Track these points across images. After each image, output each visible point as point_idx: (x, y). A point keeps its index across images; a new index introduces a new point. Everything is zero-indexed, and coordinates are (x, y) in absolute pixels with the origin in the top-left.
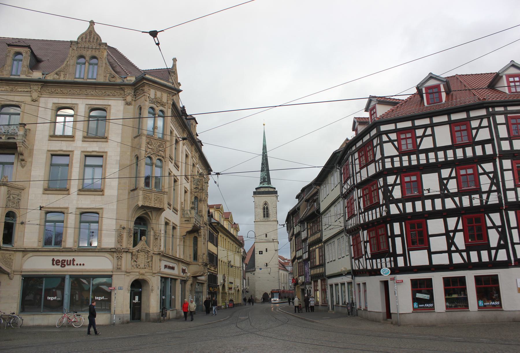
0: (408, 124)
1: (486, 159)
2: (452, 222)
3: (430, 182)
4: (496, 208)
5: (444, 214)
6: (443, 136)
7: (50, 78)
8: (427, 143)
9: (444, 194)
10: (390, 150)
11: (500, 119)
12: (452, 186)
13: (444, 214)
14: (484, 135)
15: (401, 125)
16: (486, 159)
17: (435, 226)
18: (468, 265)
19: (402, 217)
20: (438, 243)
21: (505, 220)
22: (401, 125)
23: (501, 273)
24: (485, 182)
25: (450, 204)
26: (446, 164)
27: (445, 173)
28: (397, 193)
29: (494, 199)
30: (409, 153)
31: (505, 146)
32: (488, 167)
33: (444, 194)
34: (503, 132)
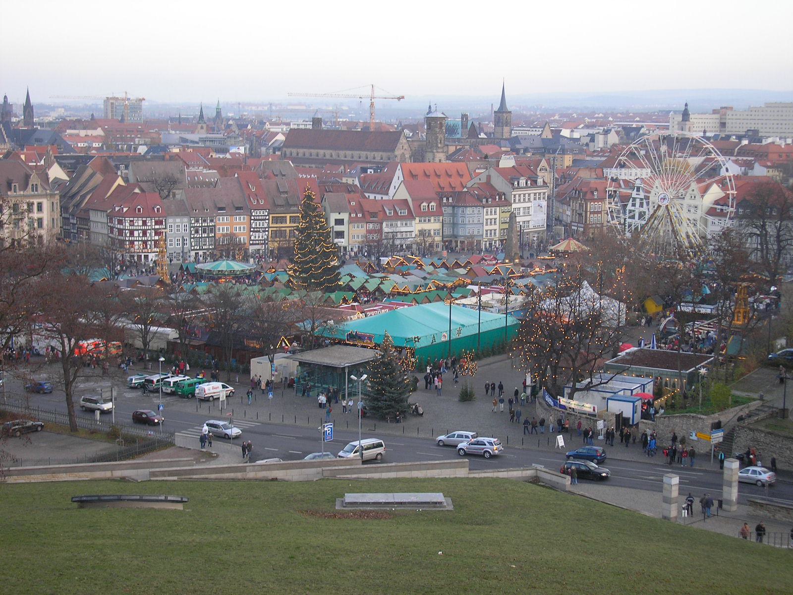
0: (132, 219)
1: (149, 229)
2: (140, 242)
3: (136, 233)
4: (150, 241)
5: (139, 241)
6: (140, 223)
7: (26, 193)
8: (136, 224)
9: (139, 236)
10: (127, 224)
11: (153, 221)
12: (141, 235)
13: (139, 241)
14: (149, 224)
15: (131, 219)
16: (149, 229)
17: (136, 243)
18: (142, 252)
19: (129, 240)
20: (137, 247)
21: (151, 243)
22: (131, 219)
23: (149, 254)
24: (148, 235)
25: (140, 239)
26: (140, 230)
27: (140, 231)
28: (128, 235)
29: (149, 239)
30: (132, 226)
31: (153, 227)
32: (149, 231)
33: (139, 236)
34: (153, 224)
